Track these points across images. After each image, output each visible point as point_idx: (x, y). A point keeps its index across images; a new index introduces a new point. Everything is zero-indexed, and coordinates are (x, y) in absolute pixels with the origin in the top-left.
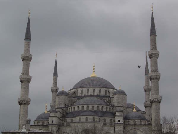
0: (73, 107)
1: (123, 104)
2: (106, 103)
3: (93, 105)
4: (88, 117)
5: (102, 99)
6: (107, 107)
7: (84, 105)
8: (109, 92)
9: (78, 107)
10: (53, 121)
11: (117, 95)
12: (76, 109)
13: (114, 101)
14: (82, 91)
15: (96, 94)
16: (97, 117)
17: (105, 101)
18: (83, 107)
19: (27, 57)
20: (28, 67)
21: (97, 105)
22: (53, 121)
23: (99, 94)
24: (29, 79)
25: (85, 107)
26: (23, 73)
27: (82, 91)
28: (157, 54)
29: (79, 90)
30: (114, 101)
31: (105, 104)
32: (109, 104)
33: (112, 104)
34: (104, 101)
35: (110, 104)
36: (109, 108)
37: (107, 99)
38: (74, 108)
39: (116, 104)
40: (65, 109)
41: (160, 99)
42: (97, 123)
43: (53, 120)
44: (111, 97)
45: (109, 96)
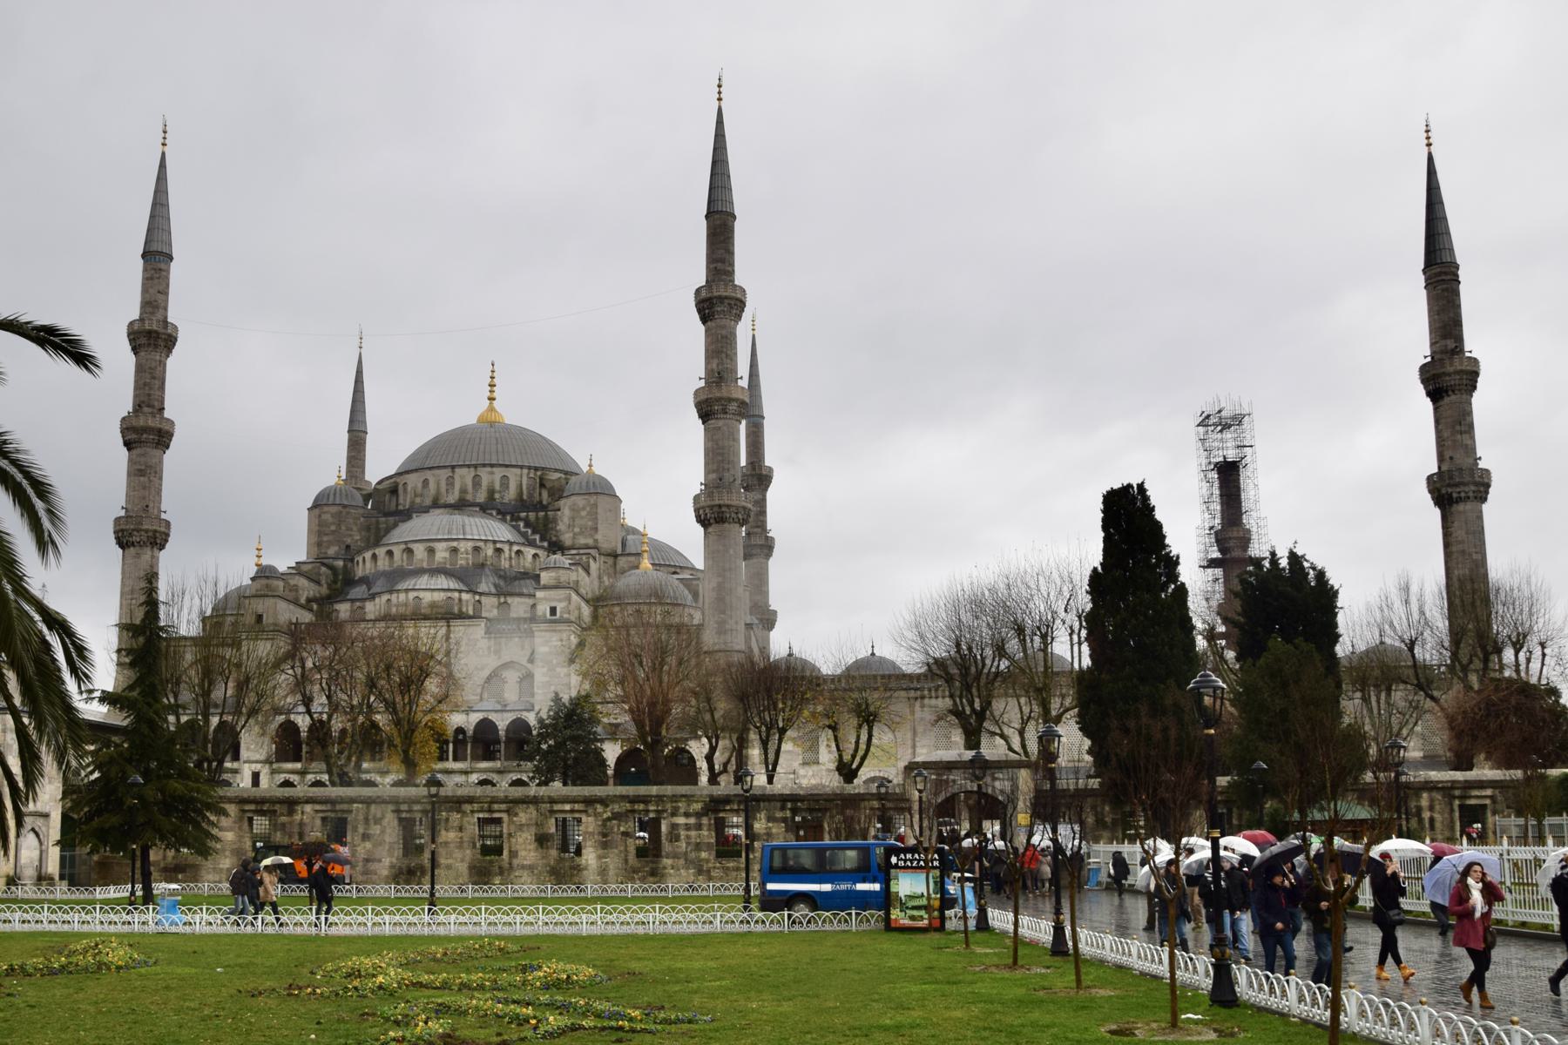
0: (368, 555)
2: (524, 535)
3: (455, 544)
4: (421, 594)
6: (518, 552)
7: (414, 547)
9: (390, 553)
12: (383, 564)
14: (426, 483)
15: (481, 497)
16: (465, 596)
17: (522, 524)
18: (409, 551)
21: (470, 545)
24: (160, 430)
25: (420, 550)
26: (138, 407)
27: (426, 483)
29: (414, 481)
31: (522, 540)
32: (537, 537)
34: (516, 528)
35: (542, 539)
36: (529, 558)
37: (532, 515)
38: (374, 557)
39: (567, 539)
42: (467, 622)
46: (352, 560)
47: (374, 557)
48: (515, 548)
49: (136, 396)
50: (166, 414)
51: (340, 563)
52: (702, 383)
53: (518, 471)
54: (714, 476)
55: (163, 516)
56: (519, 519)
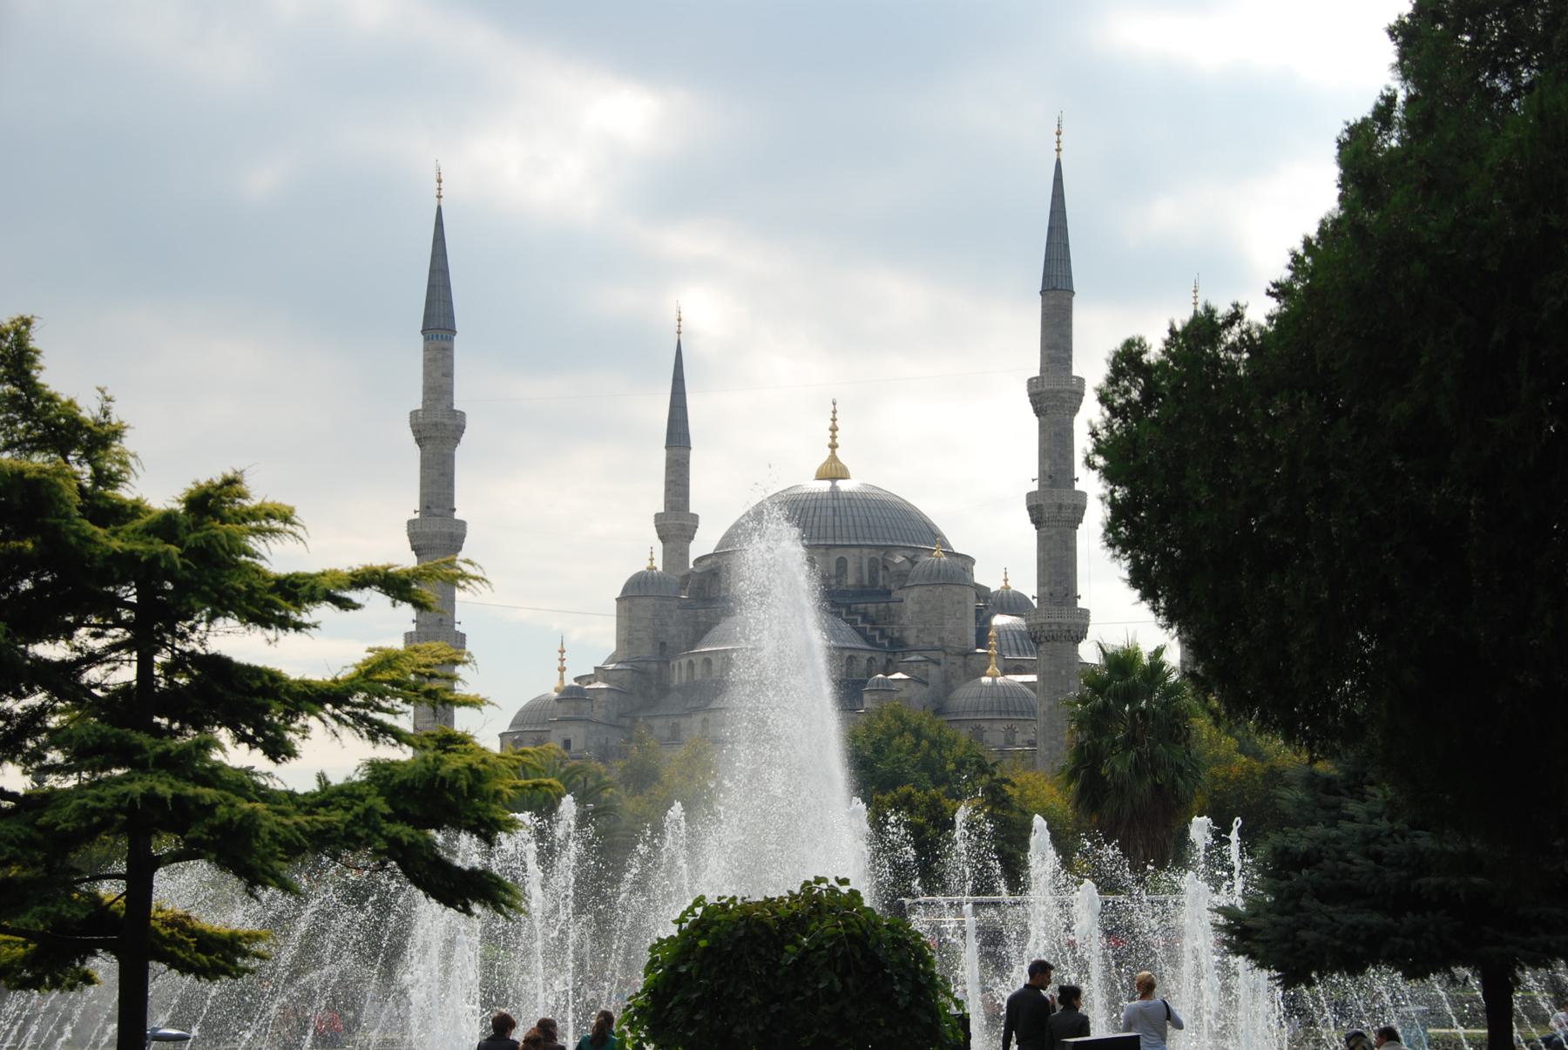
1: (945, 634)
5: (844, 611)
6: (850, 657)
8: (886, 568)
10: (567, 744)
11: (916, 590)
13: (905, 621)
19: (436, 425)
20: (442, 475)
22: (567, 744)
23: (833, 582)
24: (451, 535)
26: (426, 508)
28: (1066, 395)
30: (905, 621)
32: (877, 633)
33: (897, 635)
34: (852, 623)
35: (883, 635)
36: (865, 662)
38: (691, 664)
39: (911, 636)
40: (654, 666)
41: (1077, 625)
43: (571, 736)
44: (894, 596)
45: (889, 593)
46: (668, 663)
47: (691, 664)
48: (847, 653)
49: (422, 495)
50: (458, 515)
51: (654, 666)
52: (1035, 487)
53: (856, 551)
54: (1046, 589)
55: (457, 628)
56: (856, 613)
